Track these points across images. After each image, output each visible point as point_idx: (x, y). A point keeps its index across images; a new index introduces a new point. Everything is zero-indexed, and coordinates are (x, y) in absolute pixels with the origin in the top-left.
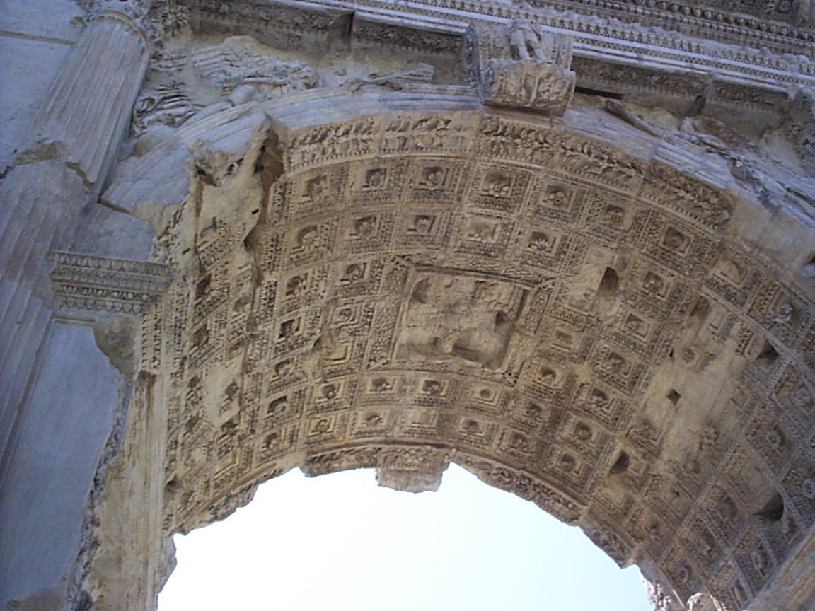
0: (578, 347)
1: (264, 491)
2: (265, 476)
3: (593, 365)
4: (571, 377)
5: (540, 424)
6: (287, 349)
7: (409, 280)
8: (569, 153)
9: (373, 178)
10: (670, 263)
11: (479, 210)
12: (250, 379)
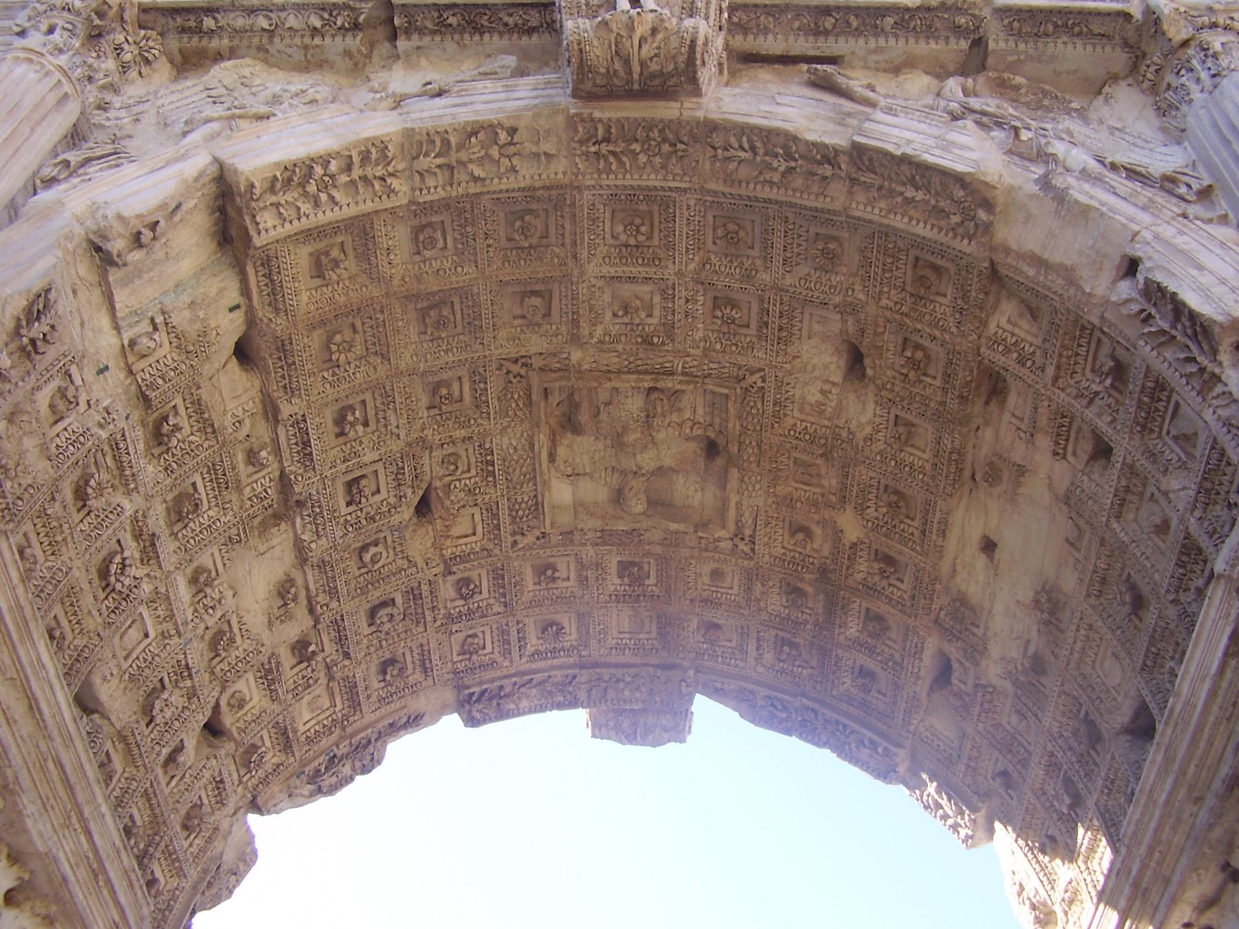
0: (834, 482)
1: (398, 750)
2: (391, 725)
3: (861, 509)
5: (811, 620)
6: (364, 522)
7: (534, 397)
9: (421, 238)
10: (927, 317)
11: (612, 270)
12: (316, 573)
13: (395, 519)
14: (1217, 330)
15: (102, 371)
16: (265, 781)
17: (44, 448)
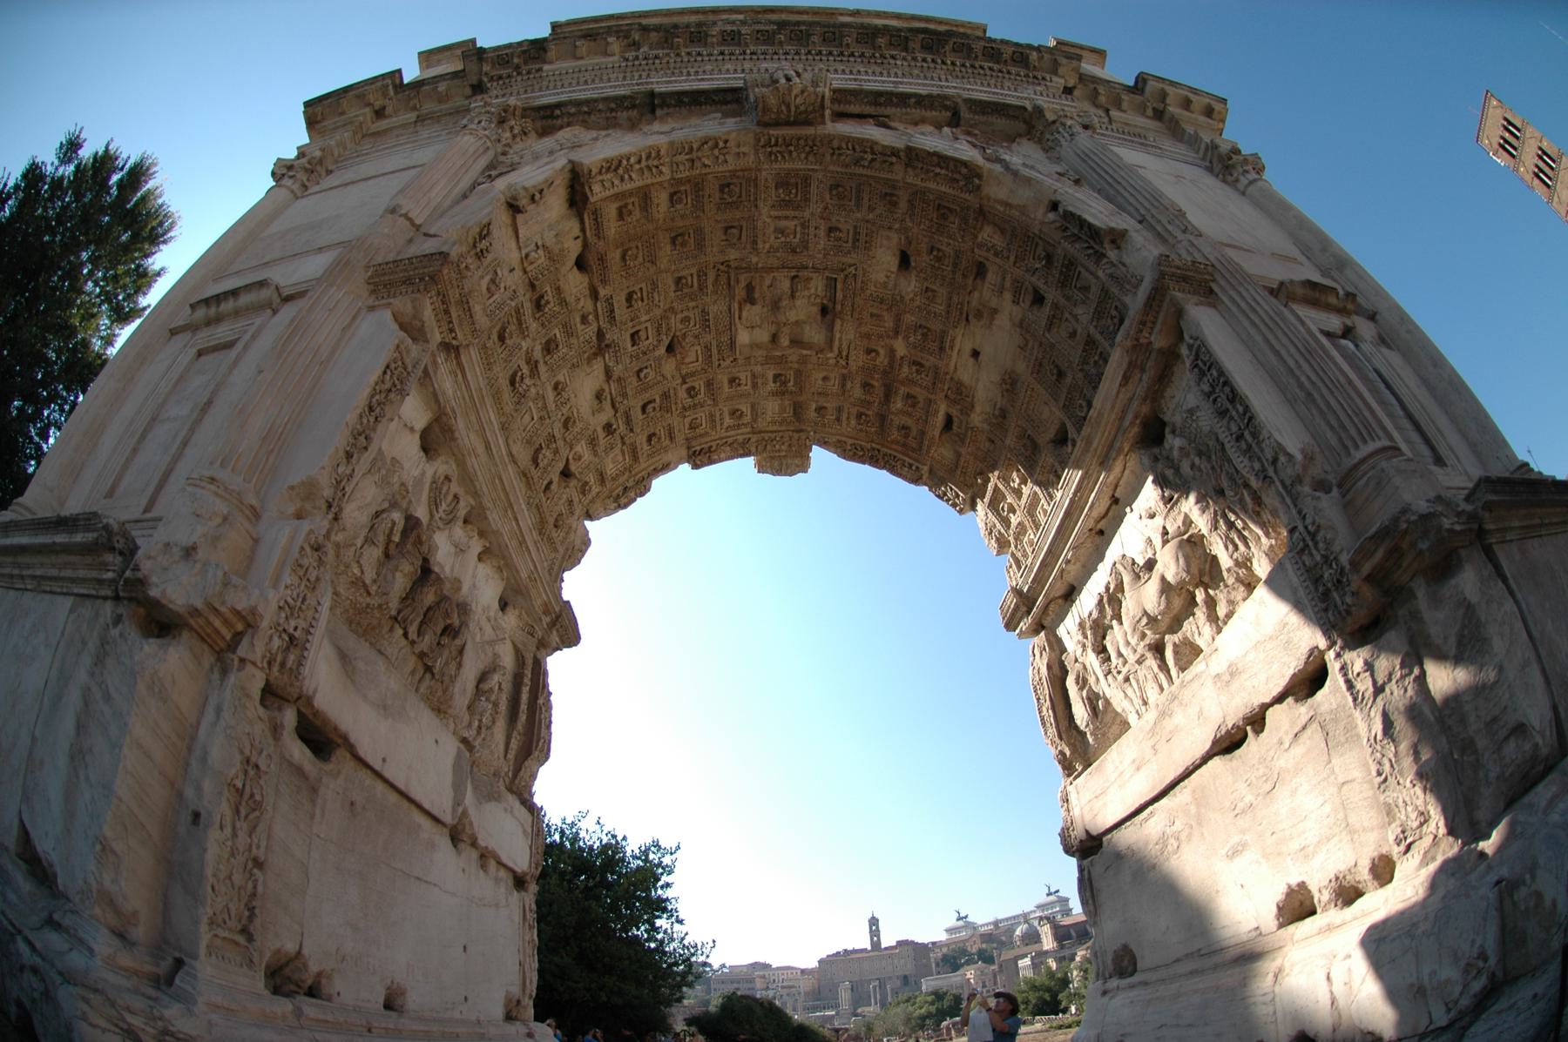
0: (891, 324)
1: (659, 484)
3: (906, 338)
4: (892, 351)
7: (732, 283)
8: (837, 152)
13: (657, 353)
14: (1102, 232)
15: (512, 270)
16: (592, 501)
17: (484, 310)
